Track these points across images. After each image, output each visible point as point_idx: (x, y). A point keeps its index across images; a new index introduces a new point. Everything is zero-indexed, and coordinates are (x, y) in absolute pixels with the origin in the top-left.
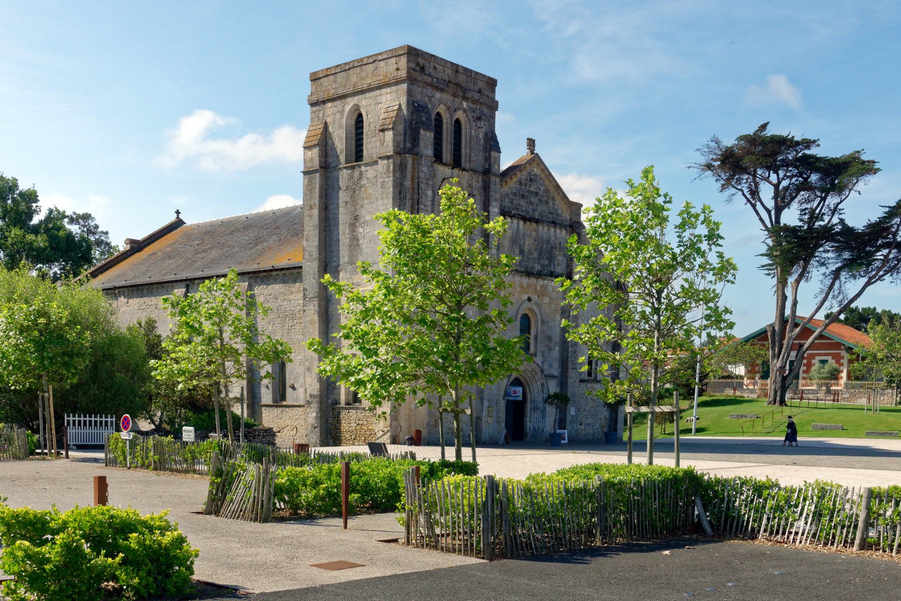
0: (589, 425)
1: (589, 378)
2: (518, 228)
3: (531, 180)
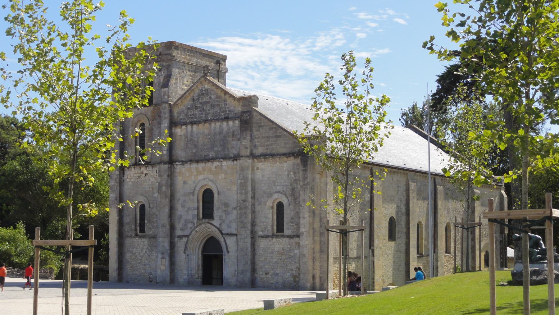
0: (277, 274)
2: (192, 130)
3: (203, 94)
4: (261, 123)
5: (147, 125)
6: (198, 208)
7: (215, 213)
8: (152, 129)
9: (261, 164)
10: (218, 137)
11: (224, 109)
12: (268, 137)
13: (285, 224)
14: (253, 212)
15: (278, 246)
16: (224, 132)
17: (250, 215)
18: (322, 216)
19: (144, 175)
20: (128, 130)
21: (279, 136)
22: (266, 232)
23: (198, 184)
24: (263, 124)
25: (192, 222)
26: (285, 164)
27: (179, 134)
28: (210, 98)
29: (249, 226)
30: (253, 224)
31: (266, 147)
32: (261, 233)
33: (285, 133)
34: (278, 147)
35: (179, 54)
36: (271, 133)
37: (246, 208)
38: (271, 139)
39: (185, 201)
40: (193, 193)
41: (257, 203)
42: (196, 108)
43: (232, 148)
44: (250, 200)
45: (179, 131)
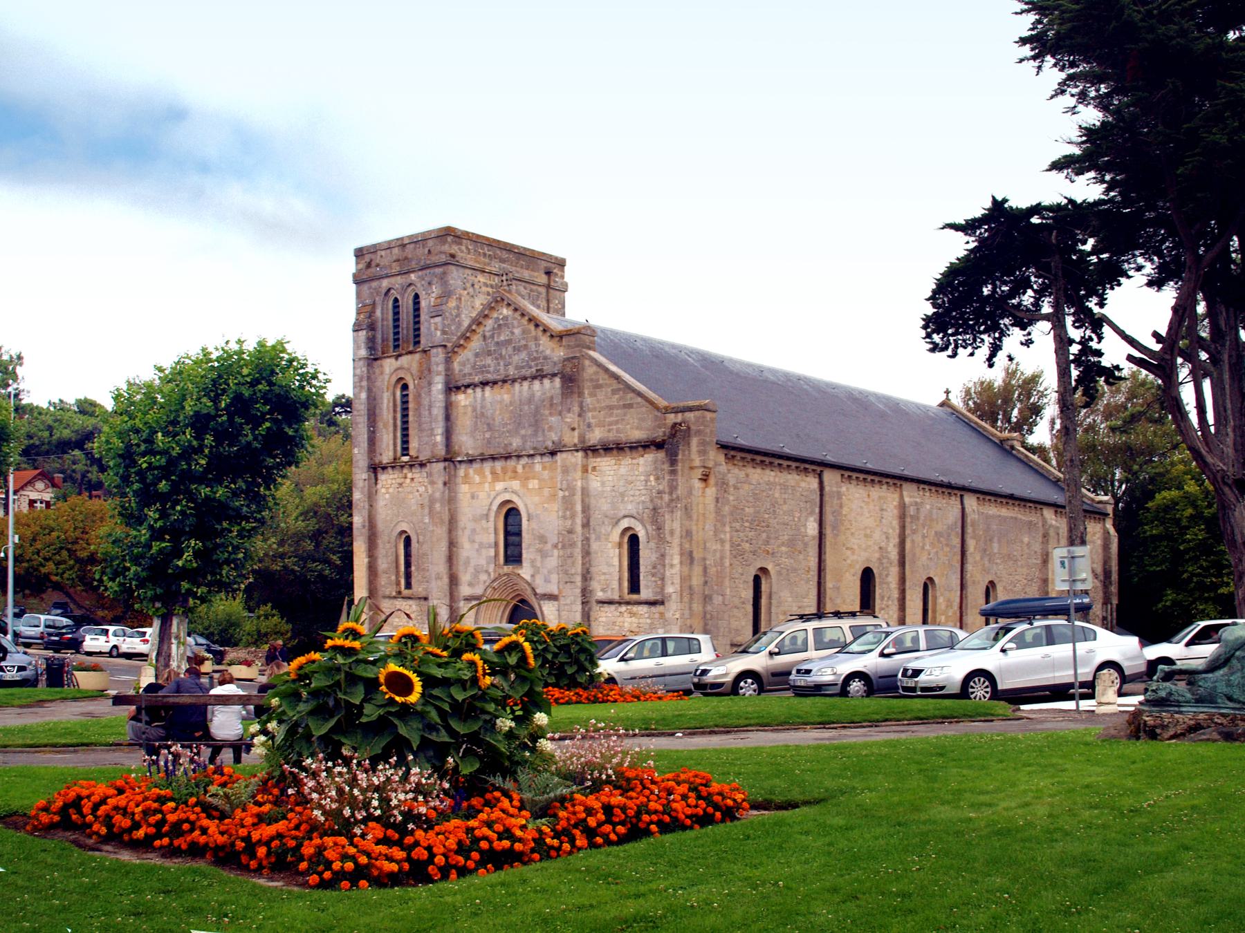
1: (635, 597)
2: (483, 395)
4: (598, 380)
5: (411, 386)
6: (496, 544)
7: (525, 555)
8: (419, 395)
9: (599, 459)
10: (526, 407)
11: (535, 354)
12: (611, 408)
13: (641, 578)
14: (587, 553)
15: (629, 620)
16: (536, 399)
17: (580, 558)
18: (708, 562)
19: (408, 481)
20: (382, 398)
21: (630, 406)
22: (609, 593)
23: (495, 498)
24: (601, 382)
25: (487, 571)
26: (641, 460)
27: (463, 403)
28: (513, 333)
29: (578, 579)
30: (586, 576)
31: (607, 428)
32: (600, 595)
33: (639, 399)
34: (628, 427)
35: (462, 252)
36: (614, 400)
37: (573, 545)
38: (615, 411)
39: (474, 531)
40: (487, 516)
41: (593, 537)
42: (489, 353)
43: (551, 428)
44: (579, 529)
45: (461, 399)
